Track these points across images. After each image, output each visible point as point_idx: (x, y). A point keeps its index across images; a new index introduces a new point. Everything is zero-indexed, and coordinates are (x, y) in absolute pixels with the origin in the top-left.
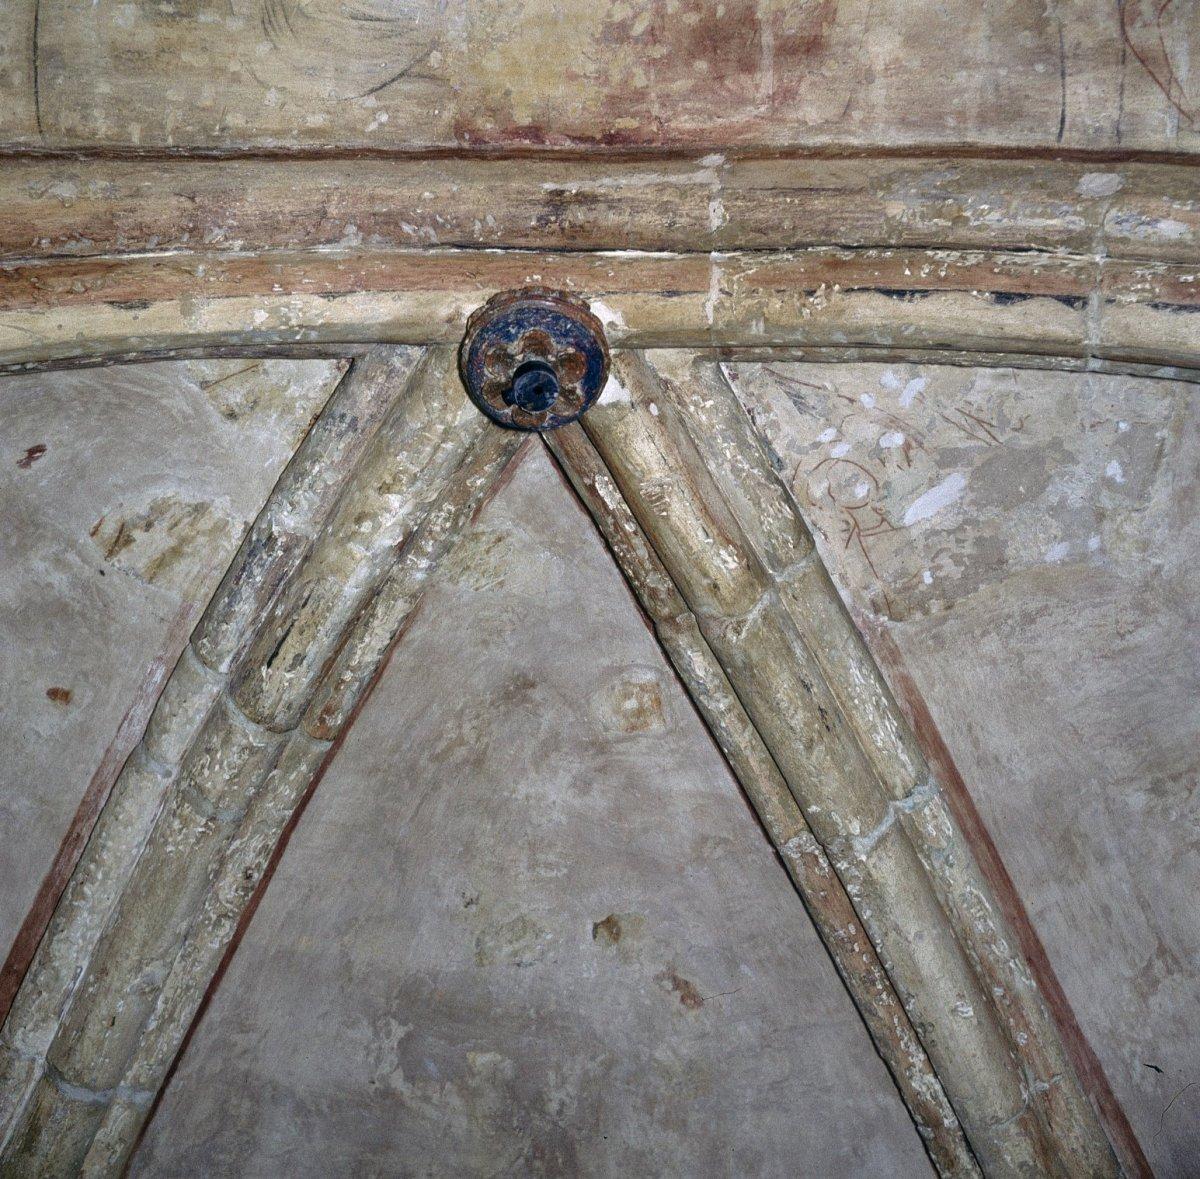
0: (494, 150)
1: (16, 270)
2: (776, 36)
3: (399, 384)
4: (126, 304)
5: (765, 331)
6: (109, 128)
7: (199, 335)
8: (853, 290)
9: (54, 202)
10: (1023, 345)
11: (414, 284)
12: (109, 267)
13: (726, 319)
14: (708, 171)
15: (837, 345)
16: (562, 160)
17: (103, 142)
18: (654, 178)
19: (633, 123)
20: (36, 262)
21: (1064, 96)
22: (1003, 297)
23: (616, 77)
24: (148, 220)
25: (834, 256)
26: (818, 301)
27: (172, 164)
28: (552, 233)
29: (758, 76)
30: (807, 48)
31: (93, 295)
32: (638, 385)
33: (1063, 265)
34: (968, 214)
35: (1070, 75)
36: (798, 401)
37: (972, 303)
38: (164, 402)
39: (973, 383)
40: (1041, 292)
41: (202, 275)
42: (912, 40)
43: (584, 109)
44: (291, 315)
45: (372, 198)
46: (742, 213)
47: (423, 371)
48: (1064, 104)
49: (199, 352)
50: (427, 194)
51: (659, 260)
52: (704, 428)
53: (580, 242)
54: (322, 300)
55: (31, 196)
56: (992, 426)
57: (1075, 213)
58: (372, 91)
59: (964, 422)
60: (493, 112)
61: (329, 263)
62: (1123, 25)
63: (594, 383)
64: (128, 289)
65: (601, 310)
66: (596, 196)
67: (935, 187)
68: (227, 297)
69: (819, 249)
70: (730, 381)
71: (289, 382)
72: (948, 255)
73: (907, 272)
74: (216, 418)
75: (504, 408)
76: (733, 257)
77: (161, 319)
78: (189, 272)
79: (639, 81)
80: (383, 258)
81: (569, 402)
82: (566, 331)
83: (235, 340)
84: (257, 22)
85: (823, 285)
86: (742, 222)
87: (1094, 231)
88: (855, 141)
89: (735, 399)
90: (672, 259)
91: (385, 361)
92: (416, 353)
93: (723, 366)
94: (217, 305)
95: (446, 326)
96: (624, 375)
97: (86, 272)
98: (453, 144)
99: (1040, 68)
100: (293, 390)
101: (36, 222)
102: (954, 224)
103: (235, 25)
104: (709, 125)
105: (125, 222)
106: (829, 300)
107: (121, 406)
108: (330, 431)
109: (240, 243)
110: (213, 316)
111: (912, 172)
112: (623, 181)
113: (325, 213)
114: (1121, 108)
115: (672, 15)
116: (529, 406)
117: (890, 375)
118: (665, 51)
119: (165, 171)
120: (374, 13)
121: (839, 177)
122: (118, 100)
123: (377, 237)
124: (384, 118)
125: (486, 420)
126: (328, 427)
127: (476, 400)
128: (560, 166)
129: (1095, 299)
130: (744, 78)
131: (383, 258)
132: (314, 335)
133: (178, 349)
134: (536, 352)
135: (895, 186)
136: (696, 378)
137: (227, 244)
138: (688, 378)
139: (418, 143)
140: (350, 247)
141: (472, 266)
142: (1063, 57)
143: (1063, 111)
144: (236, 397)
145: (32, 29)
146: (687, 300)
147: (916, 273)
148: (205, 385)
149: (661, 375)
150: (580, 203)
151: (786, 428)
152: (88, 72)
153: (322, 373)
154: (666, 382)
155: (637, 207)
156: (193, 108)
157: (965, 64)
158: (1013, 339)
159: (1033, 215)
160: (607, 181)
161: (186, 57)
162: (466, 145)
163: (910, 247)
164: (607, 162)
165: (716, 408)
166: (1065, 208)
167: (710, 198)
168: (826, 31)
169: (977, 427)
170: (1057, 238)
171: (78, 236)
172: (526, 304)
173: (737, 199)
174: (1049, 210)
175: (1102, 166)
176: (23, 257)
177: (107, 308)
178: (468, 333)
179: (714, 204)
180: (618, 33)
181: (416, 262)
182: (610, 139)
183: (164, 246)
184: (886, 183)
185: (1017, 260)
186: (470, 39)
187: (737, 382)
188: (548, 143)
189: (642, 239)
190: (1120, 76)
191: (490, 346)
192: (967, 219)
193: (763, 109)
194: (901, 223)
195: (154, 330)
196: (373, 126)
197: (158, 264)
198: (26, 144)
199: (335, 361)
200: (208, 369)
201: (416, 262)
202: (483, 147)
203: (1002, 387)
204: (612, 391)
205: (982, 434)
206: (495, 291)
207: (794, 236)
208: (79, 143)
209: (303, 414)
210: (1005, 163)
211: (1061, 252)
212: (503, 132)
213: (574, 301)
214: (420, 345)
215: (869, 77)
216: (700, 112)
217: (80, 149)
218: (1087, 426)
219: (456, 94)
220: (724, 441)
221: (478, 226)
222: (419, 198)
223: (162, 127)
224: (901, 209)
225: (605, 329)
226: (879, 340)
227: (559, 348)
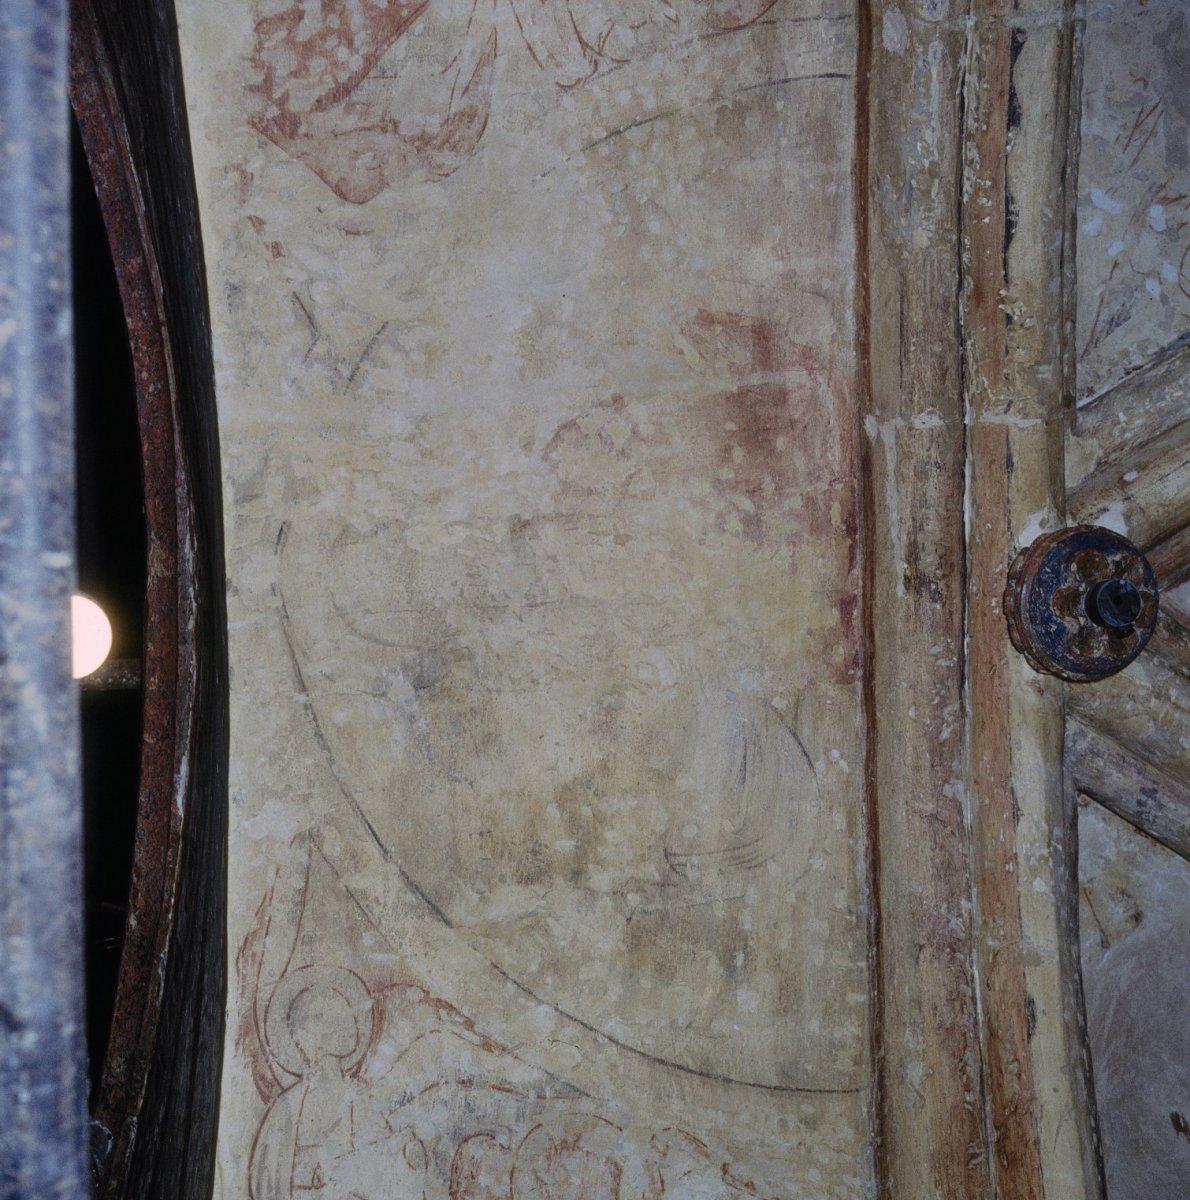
0: (864, 645)
1: (997, 1128)
2: (753, 370)
3: (1105, 744)
4: (1030, 1021)
5: (1049, 363)
6: (852, 1023)
7: (1060, 949)
8: (1006, 275)
9: (928, 1084)
10: (1063, 90)
11: (1003, 728)
12: (992, 1034)
13: (1036, 406)
14: (883, 431)
15: (1062, 286)
16: (873, 578)
17: (866, 1030)
18: (891, 484)
19: (836, 507)
20: (988, 1108)
21: (808, 77)
22: (1014, 118)
23: (792, 526)
24: (943, 993)
25: (969, 298)
26: (1017, 311)
27: (885, 964)
28: (948, 586)
29: (790, 386)
30: (763, 337)
31: (1021, 1054)
32: (1105, 493)
33: (978, 58)
34: (926, 163)
35: (787, 74)
36: (1114, 323)
37: (1019, 150)
38: (1124, 986)
39: (1096, 137)
40: (1007, 78)
41: (997, 943)
42: (755, 236)
43: (823, 556)
44: (1037, 854)
45: (917, 769)
46: (926, 394)
47: (1092, 719)
48: (814, 76)
49: (1074, 948)
50: (911, 713)
51: (973, 478)
52: (1149, 422)
53: (956, 558)
54: (1021, 822)
55: (923, 1107)
56: (1142, 112)
57: (925, 53)
58: (811, 765)
59: (1137, 143)
60: (827, 647)
61: (982, 813)
62: (739, 28)
63: (1106, 541)
64: (1015, 1019)
65: (1027, 537)
66: (910, 544)
67: (899, 199)
68: (1020, 918)
69: (961, 313)
70: (1096, 396)
71: (1101, 857)
72: (968, 179)
73: (987, 220)
74: (1141, 934)
75: (1136, 636)
76: (971, 401)
77: (1044, 985)
78: (995, 956)
79: (796, 503)
80: (976, 759)
81: (1129, 568)
82: (1052, 572)
83: (1063, 913)
85: (1000, 306)
86: (935, 394)
87: (942, 32)
88: (851, 284)
89: (1117, 389)
90: (973, 464)
91: (1081, 758)
92: (1072, 726)
93: (1080, 404)
94: (1029, 930)
95: (1047, 695)
96: (1094, 510)
97: (999, 1059)
98: (859, 685)
99: (779, 105)
100: (1110, 852)
101: (949, 1105)
102: (936, 177)
103: (753, 895)
104: (837, 432)
105: (947, 1016)
106: (1017, 300)
107: (1129, 1032)
108: (1155, 817)
109: (963, 902)
110: (1040, 934)
111: (883, 224)
112: (894, 516)
113: (932, 815)
114: (817, 18)
115: (736, 474)
116: (1134, 609)
117: (1088, 227)
118: (768, 479)
119: (893, 971)
120: (739, 762)
121: (888, 299)
122: (825, 1012)
123: (955, 764)
124: (835, 753)
125: (1143, 654)
126: (1151, 818)
127: (1126, 663)
128: (879, 579)
129: (1016, 21)
130: (793, 399)
131: (976, 759)
132: (1058, 832)
133: (1071, 967)
134: (1076, 604)
135: (899, 240)
136: (1095, 432)
137: (966, 915)
138: (1095, 442)
139: (858, 720)
140: (966, 791)
141: (983, 670)
142: (770, 83)
143: (821, 76)
144: (1117, 913)
145: (763, 1090)
146: (1017, 447)
147: (987, 211)
148: (1105, 944)
149: (1092, 469)
150: (917, 559)
151: (1146, 333)
152: (800, 1040)
153: (1092, 822)
154: (1099, 464)
155: (921, 502)
156: (830, 941)
157: (777, 182)
158: (1057, 103)
159: (927, 95)
160: (894, 532)
161: (784, 944)
162: (860, 673)
163: (959, 219)
164: (874, 533)
165: (1127, 409)
166: (920, 64)
167: (911, 429)
168: (747, 322)
169: (1142, 127)
170: (950, 69)
171: (961, 1064)
172: (1025, 615)
173: (912, 401)
174: (922, 80)
175: (875, 30)
176: (983, 1121)
177: (1035, 1040)
178: (1054, 674)
179: (917, 424)
180: (753, 525)
181: (980, 725)
182: (851, 530)
183: (969, 978)
184: (895, 249)
185: (973, 106)
186: (761, 669)
187: (1096, 388)
188: (856, 592)
189: (952, 496)
190: (787, 23)
191: (1070, 651)
192: (932, 163)
193: (821, 379)
194: (936, 232)
195: (1056, 994)
196: (843, 764)
197: (988, 985)
198: (870, 1105)
199: (1079, 809)
200: (1089, 939)
201: (980, 725)
202: (861, 655)
203: (1099, 105)
204: (1113, 521)
205: (1151, 120)
206: (1009, 645)
207: (948, 340)
208: (867, 1053)
209: (1136, 844)
210: (873, 130)
211: (964, 61)
212: (847, 636)
213: (1020, 565)
214: (1064, 721)
215: (789, 276)
216: (825, 442)
217: (872, 1053)
218: (1142, 8)
219: (812, 683)
220: (1163, 399)
221: (942, 662)
222: (915, 721)
223: (850, 971)
224: (921, 232)
225: (1047, 531)
226: (1058, 243)
227: (1071, 579)
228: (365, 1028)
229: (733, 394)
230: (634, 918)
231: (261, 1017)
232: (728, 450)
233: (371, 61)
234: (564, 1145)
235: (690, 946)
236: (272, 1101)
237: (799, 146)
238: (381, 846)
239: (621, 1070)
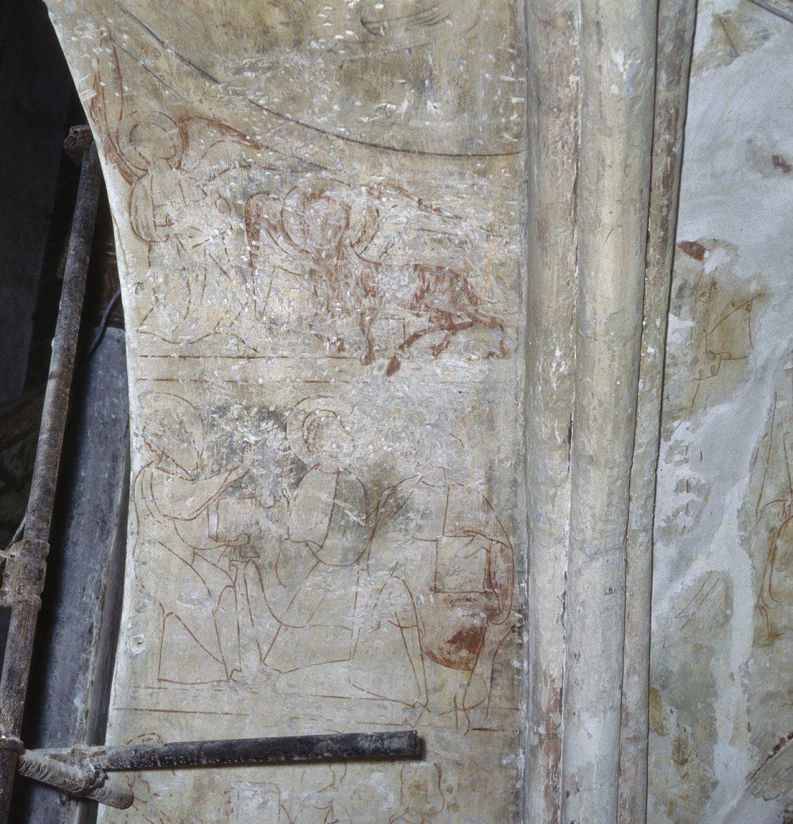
228: (178, 142)
230: (346, 65)
231: (114, 140)
234: (313, 196)
236: (134, 184)
238: (159, 40)
239: (347, 152)
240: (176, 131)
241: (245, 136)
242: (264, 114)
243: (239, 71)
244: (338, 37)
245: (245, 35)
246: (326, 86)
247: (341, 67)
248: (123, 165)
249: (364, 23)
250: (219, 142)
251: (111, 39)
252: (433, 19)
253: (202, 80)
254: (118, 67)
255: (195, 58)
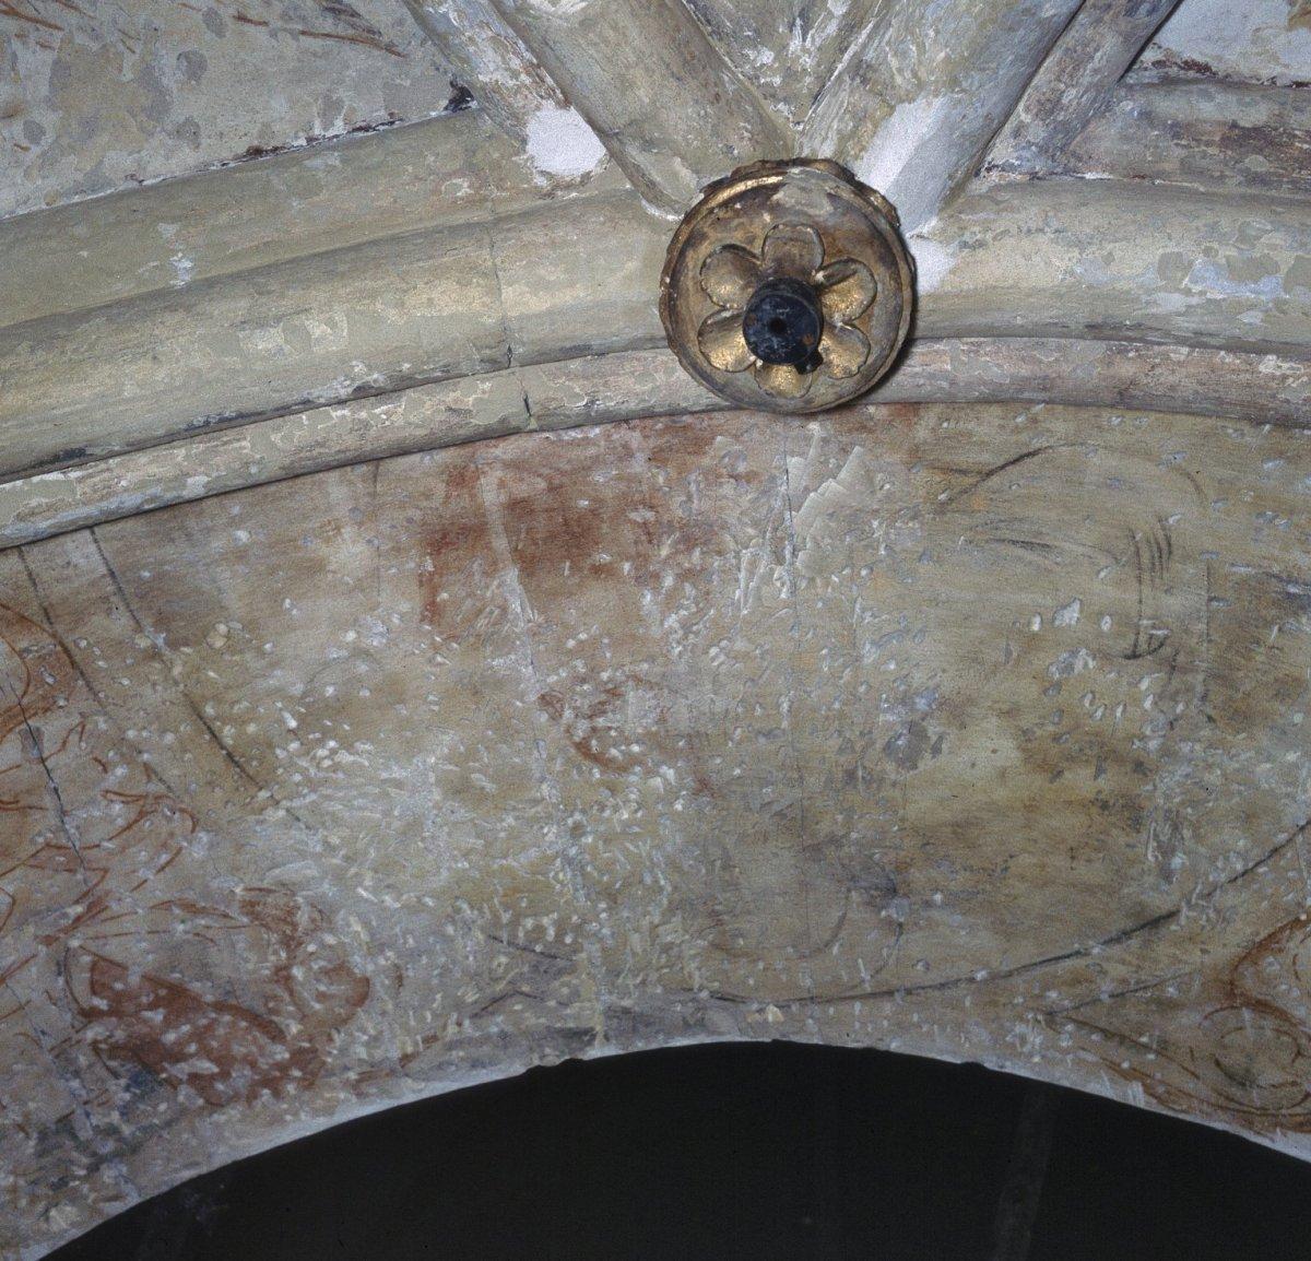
29: (503, 498)
42: (316, 567)
84: (1177, 553)
120: (1020, 552)
130: (521, 490)
228: (1269, 1023)
229: (522, 570)
232: (597, 570)
233: (220, 1007)
235: (1262, 650)
237: (189, 536)
240: (1247, 1014)
241: (1297, 920)
242: (1265, 873)
243: (1166, 874)
244: (1148, 704)
245: (1102, 837)
246: (1243, 757)
247: (1210, 719)
248: (1284, 1121)
249: (1134, 656)
250: (1294, 963)
251: (1050, 1014)
252: (1158, 544)
253: (1163, 931)
254: (1103, 1031)
255: (1121, 923)
